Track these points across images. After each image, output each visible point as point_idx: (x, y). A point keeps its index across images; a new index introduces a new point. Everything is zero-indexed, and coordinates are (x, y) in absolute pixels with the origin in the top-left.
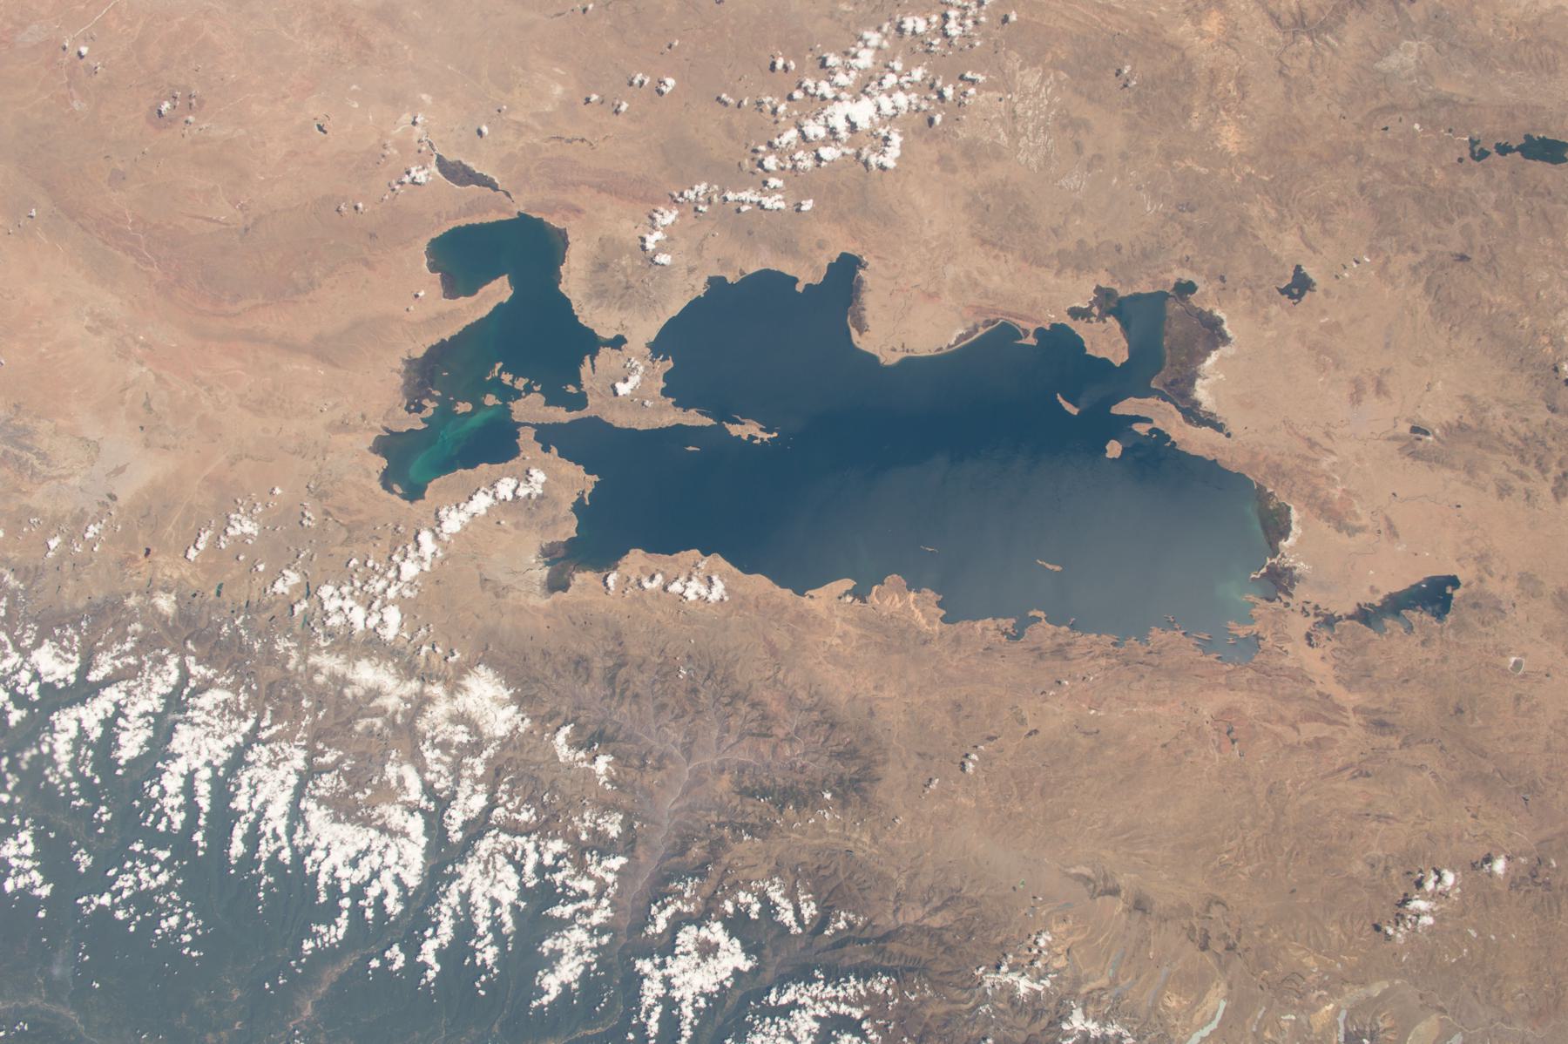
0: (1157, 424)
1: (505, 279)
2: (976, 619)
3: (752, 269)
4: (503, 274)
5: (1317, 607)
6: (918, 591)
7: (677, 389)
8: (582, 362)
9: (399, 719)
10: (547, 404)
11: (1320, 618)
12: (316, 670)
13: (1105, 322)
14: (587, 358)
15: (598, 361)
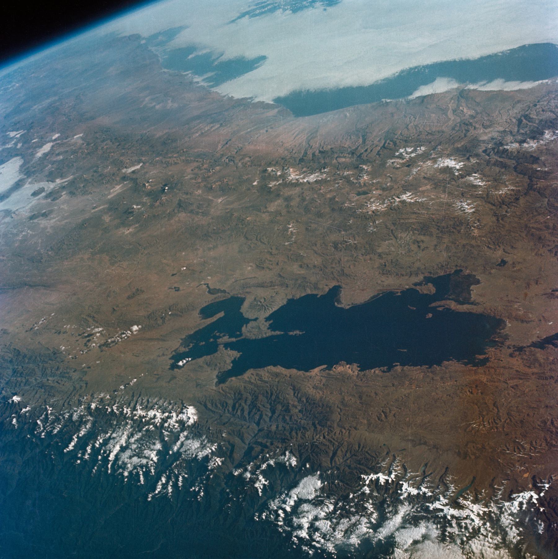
0: (446, 306)
1: (223, 312)
2: (372, 369)
3: (303, 295)
4: (222, 311)
5: (514, 346)
6: (350, 364)
7: (272, 327)
8: (243, 326)
9: (158, 424)
10: (229, 338)
11: (516, 349)
12: (135, 415)
13: (427, 285)
14: (245, 326)
15: (248, 325)
